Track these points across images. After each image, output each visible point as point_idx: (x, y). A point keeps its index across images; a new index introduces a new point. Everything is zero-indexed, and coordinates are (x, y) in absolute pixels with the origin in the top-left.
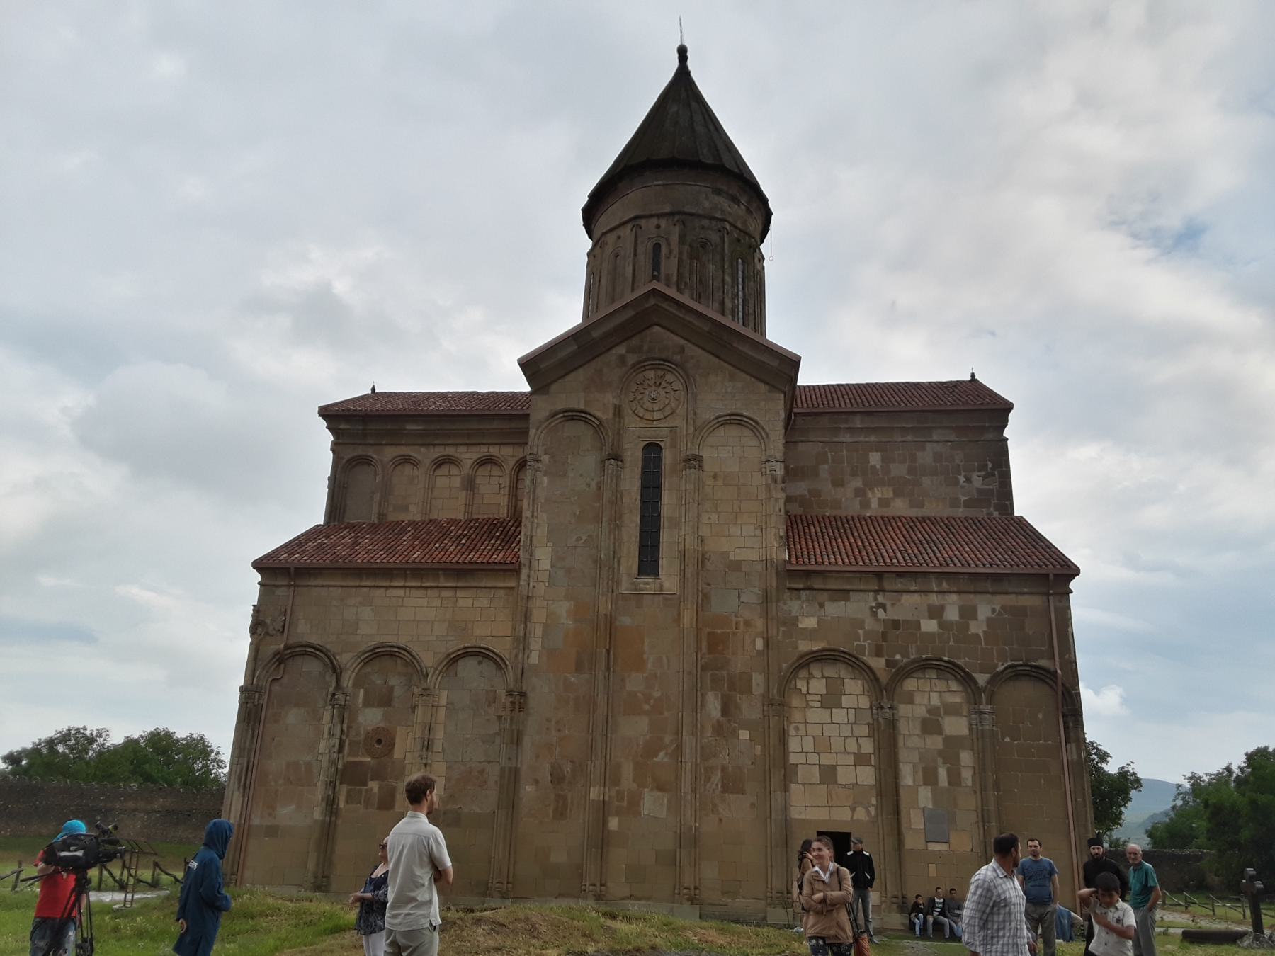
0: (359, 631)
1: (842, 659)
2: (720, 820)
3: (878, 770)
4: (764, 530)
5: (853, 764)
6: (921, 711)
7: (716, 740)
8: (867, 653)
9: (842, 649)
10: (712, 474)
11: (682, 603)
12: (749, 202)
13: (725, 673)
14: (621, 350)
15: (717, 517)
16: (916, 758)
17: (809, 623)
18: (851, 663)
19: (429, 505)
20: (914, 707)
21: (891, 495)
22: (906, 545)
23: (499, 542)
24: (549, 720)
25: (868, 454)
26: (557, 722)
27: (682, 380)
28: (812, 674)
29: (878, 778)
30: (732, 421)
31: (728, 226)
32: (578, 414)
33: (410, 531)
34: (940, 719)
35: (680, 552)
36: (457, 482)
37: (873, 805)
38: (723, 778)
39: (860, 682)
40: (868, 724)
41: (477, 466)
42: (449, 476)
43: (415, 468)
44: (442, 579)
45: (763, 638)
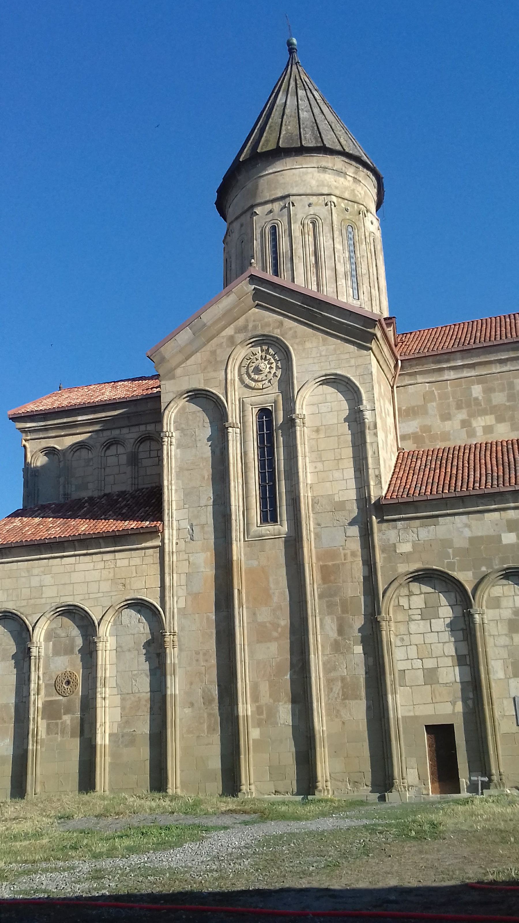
0: (43, 596)
1: (435, 576)
2: (343, 723)
3: (472, 669)
4: (362, 472)
5: (452, 665)
7: (335, 656)
8: (456, 568)
9: (434, 567)
10: (316, 428)
11: (297, 543)
12: (356, 173)
13: (338, 599)
14: (229, 331)
15: (322, 465)
17: (405, 548)
18: (444, 579)
19: (103, 482)
20: (501, 611)
21: (494, 422)
22: (495, 468)
23: (152, 508)
24: (197, 653)
25: (471, 388)
26: (205, 654)
27: (283, 351)
28: (412, 592)
29: (473, 675)
30: (328, 381)
31: (334, 199)
32: (199, 392)
33: (86, 507)
35: (293, 499)
36: (123, 459)
37: (470, 699)
38: (343, 688)
39: (453, 595)
40: (462, 630)
41: (139, 444)
42: (117, 455)
43: (90, 452)
44: (103, 544)
45: (368, 565)
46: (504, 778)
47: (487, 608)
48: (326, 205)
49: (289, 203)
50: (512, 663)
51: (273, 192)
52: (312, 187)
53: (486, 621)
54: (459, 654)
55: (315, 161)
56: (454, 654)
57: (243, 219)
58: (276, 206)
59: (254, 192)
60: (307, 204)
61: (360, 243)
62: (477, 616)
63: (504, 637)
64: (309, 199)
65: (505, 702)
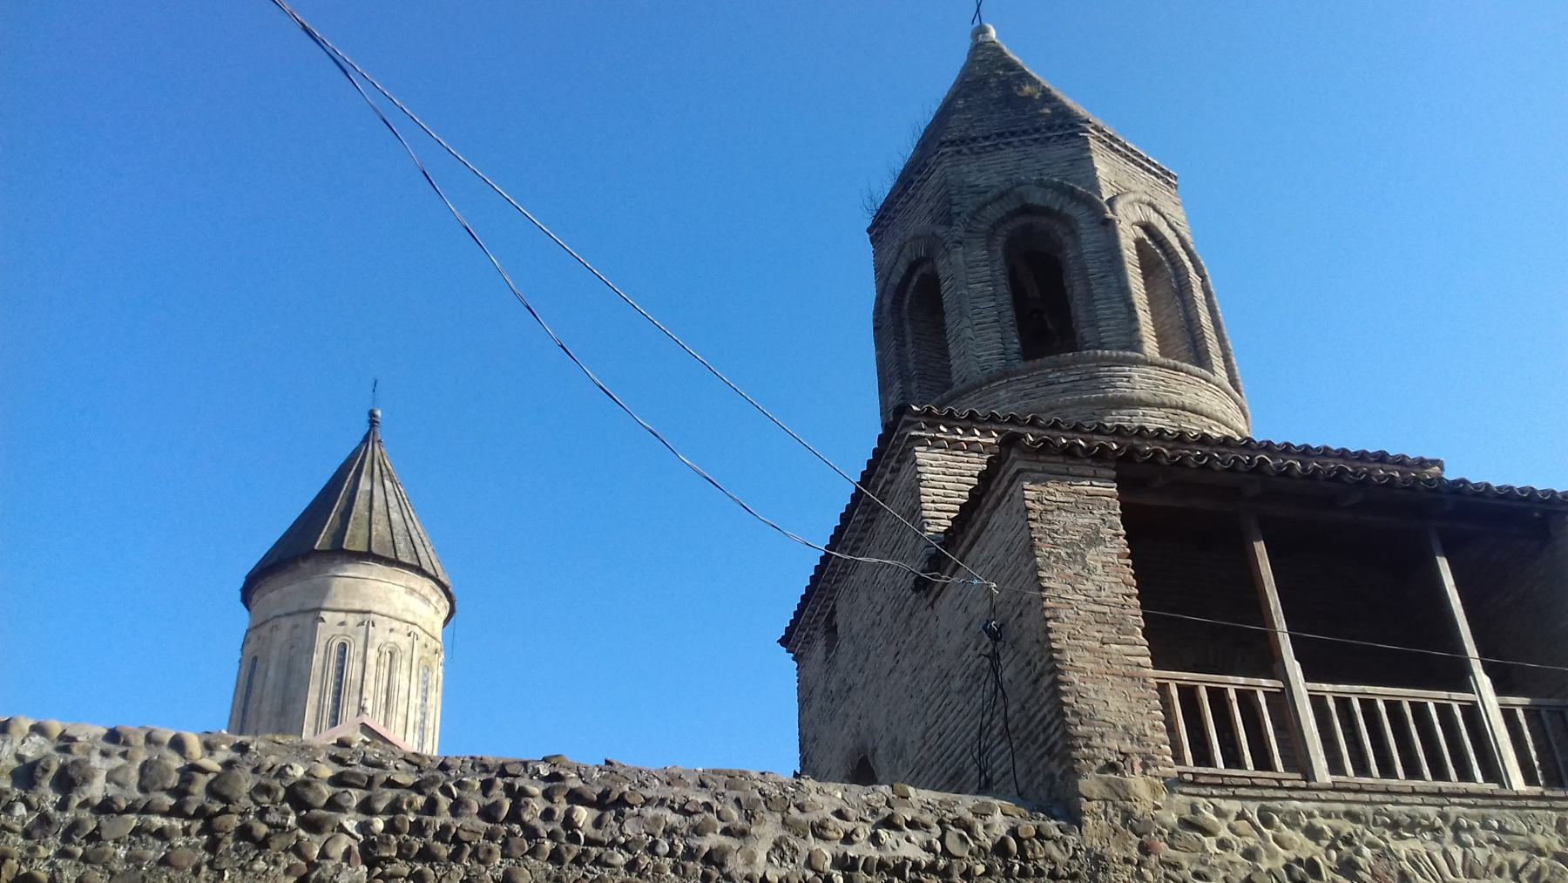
12: (438, 602)
48: (409, 635)
49: (369, 622)
51: (350, 601)
52: (396, 610)
55: (404, 579)
57: (299, 619)
58: (352, 620)
59: (324, 591)
60: (388, 627)
61: (432, 690)
64: (391, 623)
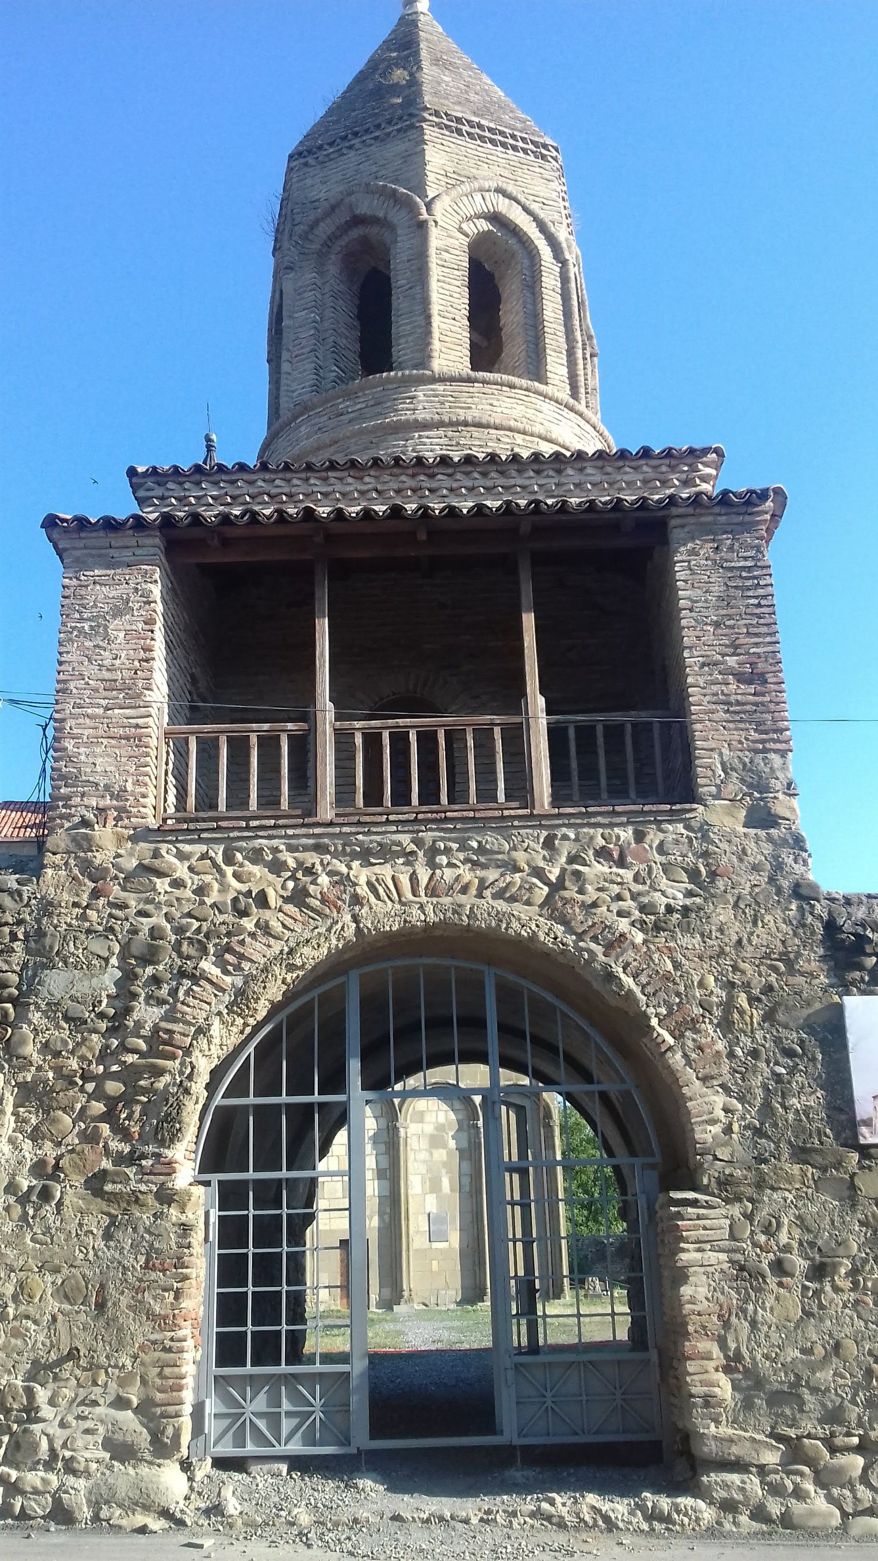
6: (429, 1129)
16: (423, 1169)
34: (445, 1135)
39: (379, 1106)
46: (413, 1293)
47: (411, 1121)
50: (430, 1179)
53: (409, 1135)
54: (380, 1167)
56: (375, 1167)
62: (401, 1130)
63: (424, 1152)
65: (420, 1217)
